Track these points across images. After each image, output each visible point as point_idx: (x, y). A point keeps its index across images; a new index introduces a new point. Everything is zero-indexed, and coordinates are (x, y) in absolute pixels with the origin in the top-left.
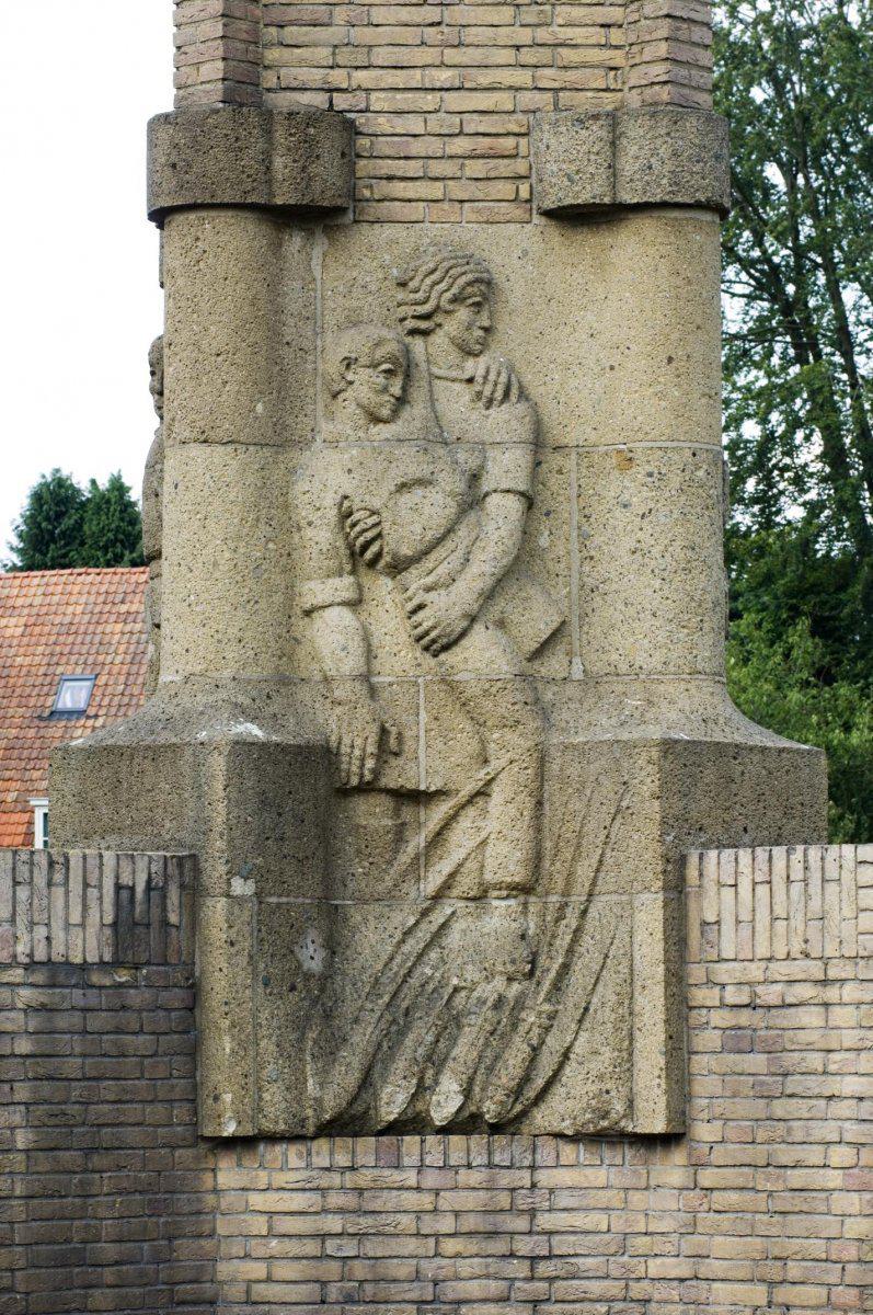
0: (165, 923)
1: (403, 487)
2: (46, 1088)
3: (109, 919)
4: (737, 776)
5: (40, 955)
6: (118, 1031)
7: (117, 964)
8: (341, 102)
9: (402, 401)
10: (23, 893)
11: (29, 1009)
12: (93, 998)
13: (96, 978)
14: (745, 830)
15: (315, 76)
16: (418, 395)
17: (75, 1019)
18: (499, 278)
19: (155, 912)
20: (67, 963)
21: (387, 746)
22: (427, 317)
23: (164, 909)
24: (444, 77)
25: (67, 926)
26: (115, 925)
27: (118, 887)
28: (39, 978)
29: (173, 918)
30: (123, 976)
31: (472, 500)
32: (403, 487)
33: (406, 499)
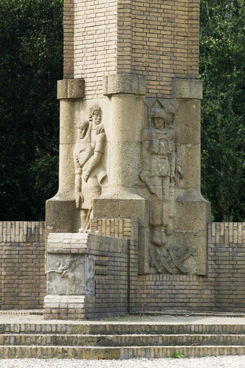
0: (39, 235)
1: (81, 151)
2: (9, 265)
3: (25, 233)
4: (117, 205)
5: (8, 240)
6: (27, 254)
7: (27, 242)
8: (84, 76)
9: (85, 134)
10: (5, 230)
11: (5, 250)
12: (21, 248)
13: (21, 245)
14: (119, 216)
15: (80, 72)
16: (88, 133)
17: (17, 252)
18: (102, 110)
19: (37, 233)
20: (15, 242)
21: (81, 200)
22: (91, 117)
23: (39, 232)
24: (95, 70)
25: (15, 235)
26: (27, 235)
27: (27, 228)
28: (8, 244)
29: (41, 233)
30: (29, 244)
31: (91, 154)
32: (81, 151)
33: (82, 153)
